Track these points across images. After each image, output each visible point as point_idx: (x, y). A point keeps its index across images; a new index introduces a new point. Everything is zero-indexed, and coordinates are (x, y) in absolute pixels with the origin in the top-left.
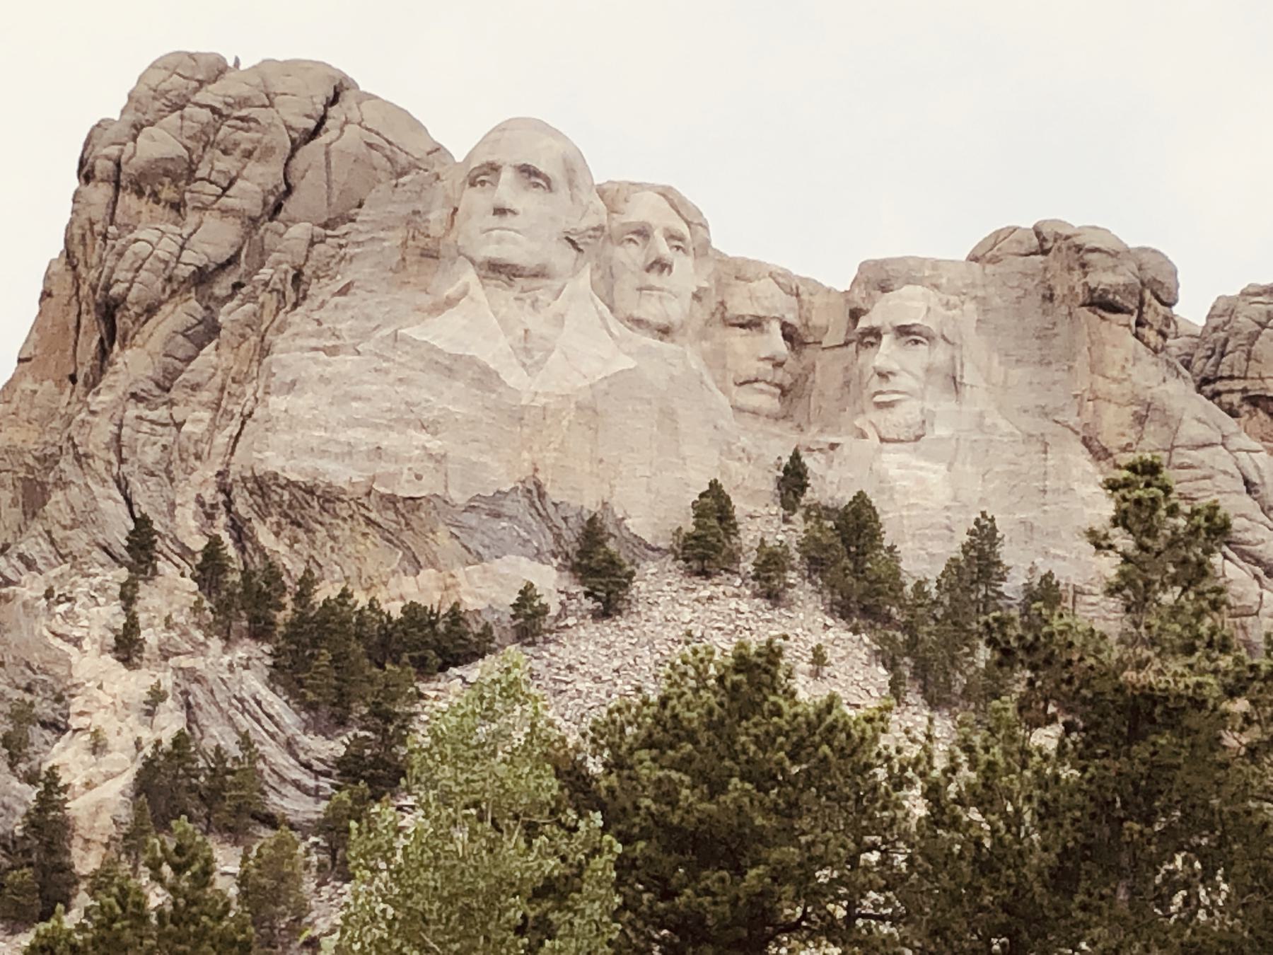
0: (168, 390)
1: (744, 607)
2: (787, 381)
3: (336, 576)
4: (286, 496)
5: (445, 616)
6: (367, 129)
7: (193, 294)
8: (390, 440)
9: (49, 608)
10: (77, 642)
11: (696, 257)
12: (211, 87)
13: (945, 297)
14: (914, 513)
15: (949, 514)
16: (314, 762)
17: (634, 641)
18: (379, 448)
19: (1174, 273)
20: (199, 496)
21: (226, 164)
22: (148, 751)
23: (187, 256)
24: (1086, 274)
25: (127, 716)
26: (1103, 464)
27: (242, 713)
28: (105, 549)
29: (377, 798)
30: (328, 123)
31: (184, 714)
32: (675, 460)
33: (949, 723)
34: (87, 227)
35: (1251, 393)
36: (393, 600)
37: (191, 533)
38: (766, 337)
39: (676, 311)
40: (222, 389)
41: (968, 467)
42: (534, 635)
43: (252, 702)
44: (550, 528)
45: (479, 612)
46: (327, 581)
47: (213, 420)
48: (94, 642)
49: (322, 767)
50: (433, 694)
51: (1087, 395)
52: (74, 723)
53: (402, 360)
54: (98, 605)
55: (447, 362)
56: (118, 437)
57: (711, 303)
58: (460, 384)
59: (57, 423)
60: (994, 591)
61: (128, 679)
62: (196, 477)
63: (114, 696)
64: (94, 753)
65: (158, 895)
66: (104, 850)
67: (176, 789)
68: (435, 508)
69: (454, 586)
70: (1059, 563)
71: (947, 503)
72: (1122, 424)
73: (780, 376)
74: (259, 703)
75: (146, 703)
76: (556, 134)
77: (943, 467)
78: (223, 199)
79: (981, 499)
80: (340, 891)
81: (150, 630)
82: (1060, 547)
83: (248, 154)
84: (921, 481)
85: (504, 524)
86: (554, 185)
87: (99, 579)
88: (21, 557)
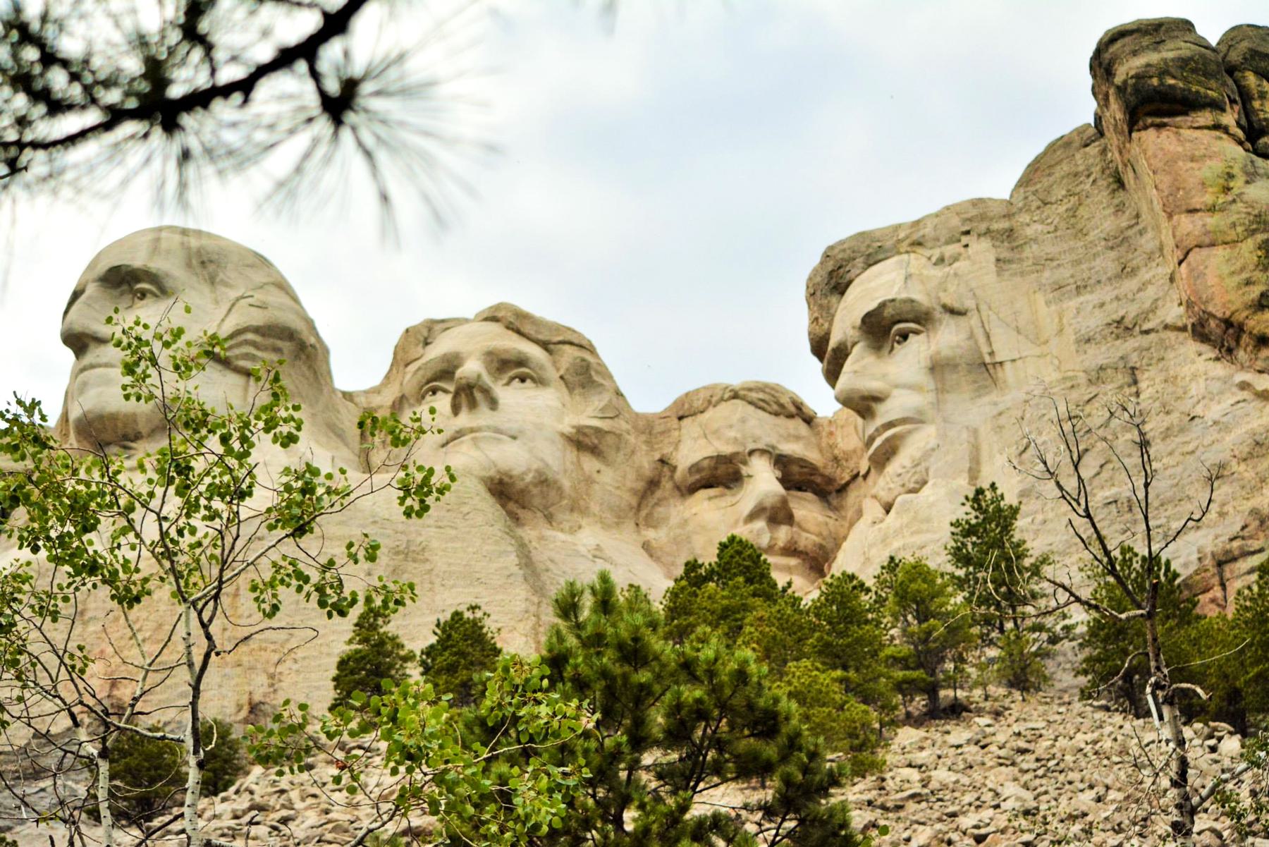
11: (570, 387)
13: (936, 253)
26: (1241, 354)
72: (1242, 269)
86: (169, 284)
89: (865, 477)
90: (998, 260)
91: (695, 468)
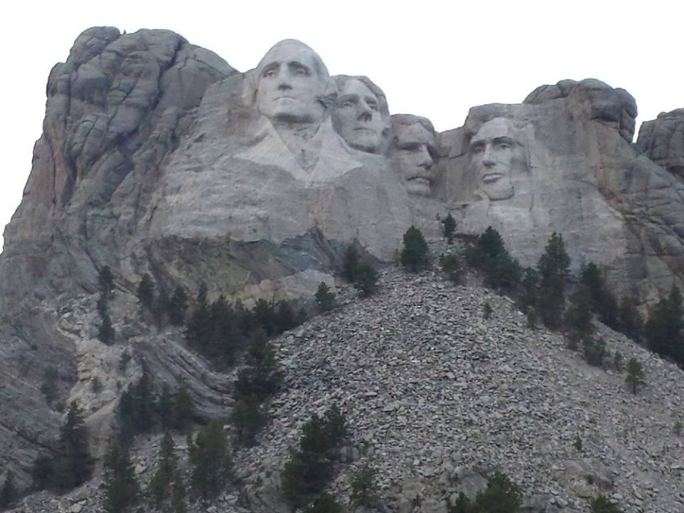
0: (109, 200)
1: (441, 286)
2: (434, 176)
3: (215, 289)
4: (182, 248)
5: (277, 304)
6: (200, 61)
7: (116, 149)
8: (236, 212)
9: (59, 316)
10: (77, 333)
12: (115, 42)
13: (517, 122)
14: (516, 234)
15: (534, 233)
16: (219, 386)
17: (385, 307)
18: (230, 217)
19: (634, 100)
20: (133, 253)
21: (128, 80)
22: (125, 388)
23: (112, 128)
24: (591, 103)
25: (110, 370)
26: (612, 202)
27: (174, 364)
28: (83, 287)
29: (262, 401)
30: (179, 59)
31: (140, 367)
32: (388, 215)
33: (562, 337)
35: (671, 165)
36: (248, 298)
37: (130, 274)
38: (420, 154)
39: (375, 139)
40: (139, 196)
41: (541, 209)
42: (329, 310)
43: (179, 358)
44: (327, 254)
45: (295, 301)
46: (209, 292)
47: (136, 212)
48: (86, 332)
49: (225, 389)
50: (279, 345)
51: (599, 166)
52: (81, 376)
53: (238, 171)
54: (86, 313)
55: (262, 170)
56: (85, 226)
57: (390, 137)
58: (270, 181)
59: (48, 225)
60: (565, 270)
61: (108, 350)
62: (129, 244)
63: (102, 360)
64: (95, 392)
65: (142, 465)
66: (107, 444)
67: (140, 411)
68: (265, 246)
69: (280, 287)
70: (594, 255)
71: (532, 228)
73: (429, 174)
74: (182, 357)
75: (121, 362)
76: (306, 46)
77: (527, 209)
78: (128, 100)
79: (550, 225)
80: (248, 453)
81: (116, 324)
82: (593, 247)
83: (138, 75)
84: (517, 217)
85: (303, 253)
87: (84, 299)
88: (36, 295)
89: (450, 159)
90: (536, 133)
91: (406, 144)
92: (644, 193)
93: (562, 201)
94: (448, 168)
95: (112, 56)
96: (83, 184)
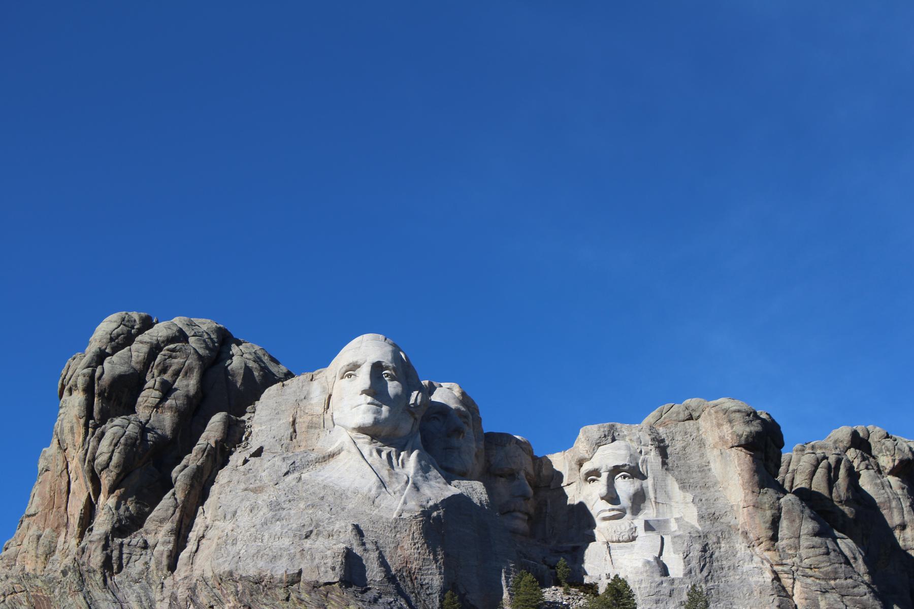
2: (532, 511)
14: (643, 586)
19: (778, 427)
24: (732, 427)
34: (75, 420)
41: (673, 555)
79: (685, 575)
92: (797, 541)
93: (698, 547)
94: (549, 501)
95: (145, 349)
96: (106, 502)
